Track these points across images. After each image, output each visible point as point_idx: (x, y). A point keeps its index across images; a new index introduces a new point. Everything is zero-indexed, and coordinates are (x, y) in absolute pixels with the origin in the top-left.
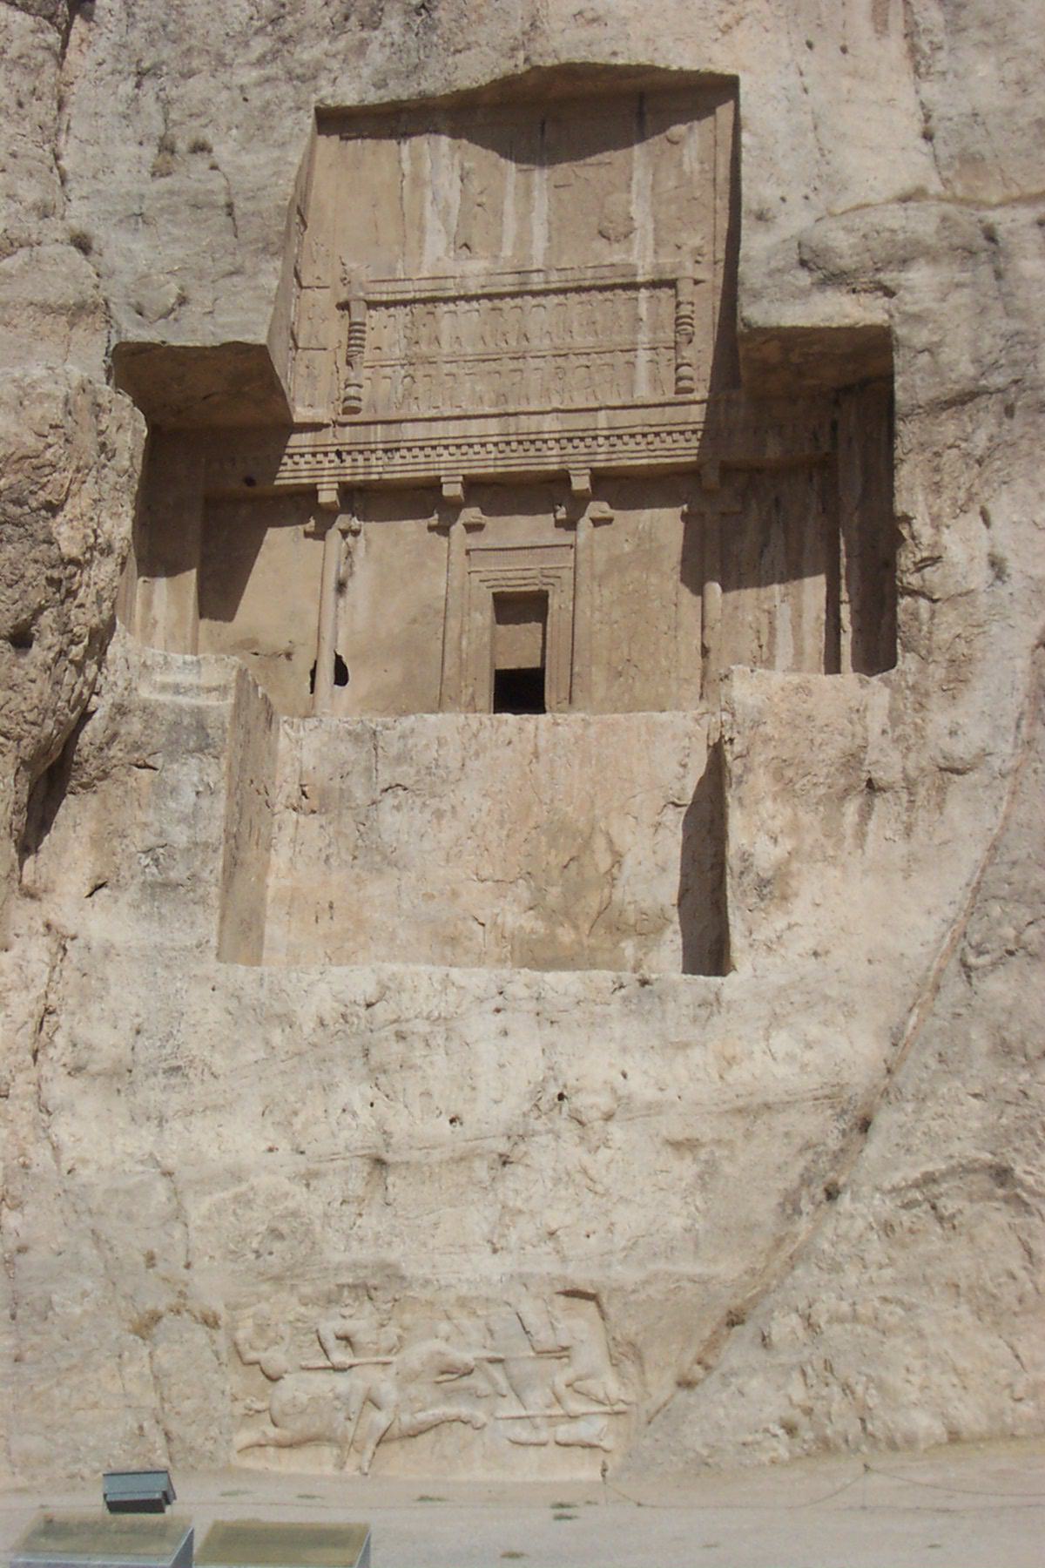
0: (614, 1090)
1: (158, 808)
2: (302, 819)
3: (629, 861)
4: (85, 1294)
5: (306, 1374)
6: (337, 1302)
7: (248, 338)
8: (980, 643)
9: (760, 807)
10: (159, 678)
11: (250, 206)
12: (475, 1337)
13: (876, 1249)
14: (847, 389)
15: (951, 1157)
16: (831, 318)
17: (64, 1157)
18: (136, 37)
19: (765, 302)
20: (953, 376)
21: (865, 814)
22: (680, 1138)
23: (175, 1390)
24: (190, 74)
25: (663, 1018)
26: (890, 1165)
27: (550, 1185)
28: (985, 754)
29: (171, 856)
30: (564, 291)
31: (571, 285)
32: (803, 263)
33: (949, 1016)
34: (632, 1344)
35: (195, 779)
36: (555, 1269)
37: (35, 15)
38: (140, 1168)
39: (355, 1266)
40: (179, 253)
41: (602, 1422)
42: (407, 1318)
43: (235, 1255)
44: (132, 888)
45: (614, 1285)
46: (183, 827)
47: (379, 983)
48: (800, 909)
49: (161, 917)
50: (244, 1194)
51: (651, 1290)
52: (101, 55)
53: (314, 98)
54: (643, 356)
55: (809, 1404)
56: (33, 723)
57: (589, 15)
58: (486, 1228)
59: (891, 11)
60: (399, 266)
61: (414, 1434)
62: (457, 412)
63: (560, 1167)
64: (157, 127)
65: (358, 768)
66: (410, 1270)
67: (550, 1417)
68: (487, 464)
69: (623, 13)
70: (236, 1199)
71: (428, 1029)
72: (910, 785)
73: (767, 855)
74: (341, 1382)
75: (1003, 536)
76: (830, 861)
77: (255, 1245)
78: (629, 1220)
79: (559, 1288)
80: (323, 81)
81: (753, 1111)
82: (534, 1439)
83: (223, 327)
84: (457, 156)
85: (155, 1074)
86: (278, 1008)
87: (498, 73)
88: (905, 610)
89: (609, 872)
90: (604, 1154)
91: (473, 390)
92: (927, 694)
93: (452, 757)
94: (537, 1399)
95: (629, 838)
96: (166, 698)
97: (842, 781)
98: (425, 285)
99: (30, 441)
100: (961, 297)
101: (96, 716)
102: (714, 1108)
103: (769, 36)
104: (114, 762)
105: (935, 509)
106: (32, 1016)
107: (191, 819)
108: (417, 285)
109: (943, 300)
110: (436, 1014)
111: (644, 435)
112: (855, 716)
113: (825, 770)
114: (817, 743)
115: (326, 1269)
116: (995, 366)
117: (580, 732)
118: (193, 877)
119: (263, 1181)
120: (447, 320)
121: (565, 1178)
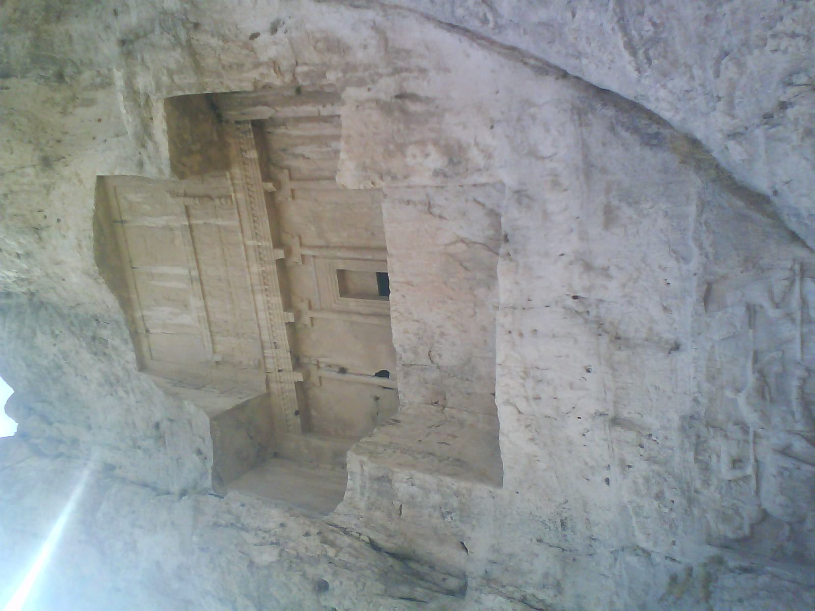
0: (571, 263)
8: (318, 35)
15: (613, 29)
16: (163, 131)
19: (162, 167)
20: (182, 61)
21: (414, 97)
24: (134, 424)
28: (375, 27)
29: (446, 504)
32: (143, 146)
35: (406, 485)
38: (618, 565)
42: (721, 417)
51: (707, 244)
54: (220, 222)
56: (364, 585)
58: (661, 355)
68: (277, 300)
70: (637, 514)
75: (261, 24)
77: (666, 510)
81: (588, 168)
85: (565, 536)
89: (467, 244)
90: (613, 271)
92: (348, 64)
100: (147, 57)
101: (372, 537)
110: (522, 374)
116: (176, 37)
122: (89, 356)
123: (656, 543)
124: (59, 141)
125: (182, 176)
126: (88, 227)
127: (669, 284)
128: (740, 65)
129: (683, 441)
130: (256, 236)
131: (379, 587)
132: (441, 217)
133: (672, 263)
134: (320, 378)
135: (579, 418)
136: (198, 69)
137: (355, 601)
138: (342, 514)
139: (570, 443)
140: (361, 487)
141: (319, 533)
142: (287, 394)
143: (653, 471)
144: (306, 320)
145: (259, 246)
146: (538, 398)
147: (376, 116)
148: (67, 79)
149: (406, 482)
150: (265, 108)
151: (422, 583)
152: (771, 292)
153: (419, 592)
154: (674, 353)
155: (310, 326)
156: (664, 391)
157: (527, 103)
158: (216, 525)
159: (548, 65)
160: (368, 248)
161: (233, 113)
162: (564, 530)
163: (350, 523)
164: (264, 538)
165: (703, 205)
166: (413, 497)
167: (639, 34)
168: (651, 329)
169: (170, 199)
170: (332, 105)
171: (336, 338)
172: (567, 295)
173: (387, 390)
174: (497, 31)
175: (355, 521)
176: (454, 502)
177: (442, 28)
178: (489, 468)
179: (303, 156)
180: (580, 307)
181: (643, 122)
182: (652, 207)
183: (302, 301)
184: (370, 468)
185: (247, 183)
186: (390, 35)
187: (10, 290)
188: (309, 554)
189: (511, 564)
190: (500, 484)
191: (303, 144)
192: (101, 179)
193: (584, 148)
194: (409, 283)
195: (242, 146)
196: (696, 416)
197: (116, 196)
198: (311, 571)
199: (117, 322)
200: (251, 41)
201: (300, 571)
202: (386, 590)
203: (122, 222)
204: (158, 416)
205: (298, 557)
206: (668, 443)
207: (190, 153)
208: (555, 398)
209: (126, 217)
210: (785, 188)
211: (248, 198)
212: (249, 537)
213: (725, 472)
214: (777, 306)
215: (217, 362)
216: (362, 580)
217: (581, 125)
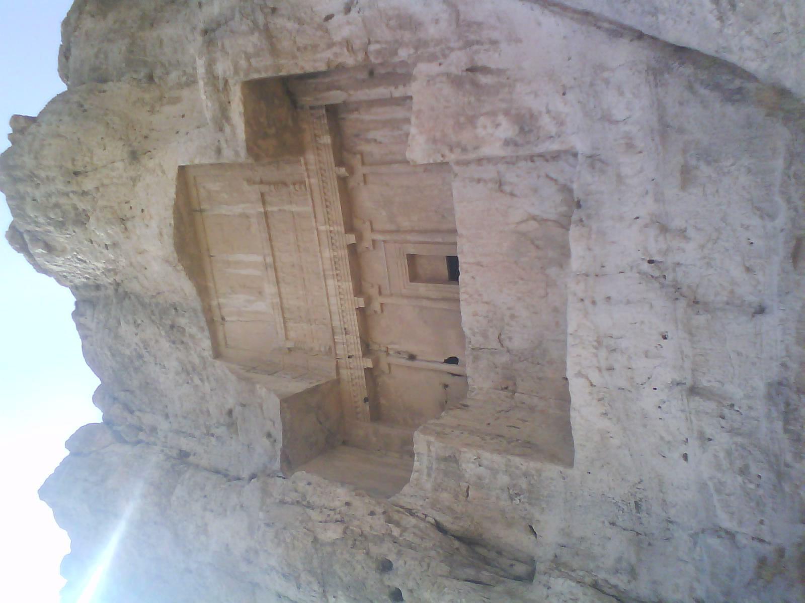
0: (646, 226)
2: (519, 390)
8: (391, 13)
10: (425, 477)
16: (240, 113)
19: (239, 149)
20: (259, 44)
21: (485, 70)
24: (208, 411)
29: (514, 486)
32: (221, 130)
54: (294, 208)
56: (429, 565)
68: (348, 285)
70: (718, 491)
79: (789, 266)
81: (664, 130)
85: (640, 518)
90: (691, 232)
100: (227, 43)
101: (438, 518)
110: (595, 344)
115: (772, 439)
116: (255, 22)
122: (168, 344)
123: (740, 523)
124: (146, 137)
127: (752, 243)
129: (770, 410)
130: (328, 221)
131: (444, 568)
132: (512, 195)
133: (755, 221)
134: (389, 365)
135: (655, 389)
136: (274, 51)
137: (420, 582)
138: (407, 496)
139: (645, 416)
140: (427, 468)
141: (384, 513)
142: (357, 380)
143: (736, 443)
144: (376, 306)
145: (331, 232)
146: (611, 369)
147: (447, 90)
148: (156, 80)
149: (473, 463)
150: (339, 92)
151: (487, 567)
153: (485, 575)
154: (759, 316)
156: (747, 357)
157: (600, 68)
158: (282, 502)
159: (623, 27)
160: (438, 231)
161: (308, 99)
162: (638, 512)
163: (417, 504)
164: (329, 515)
166: (480, 478)
169: (245, 186)
170: (404, 85)
171: (406, 323)
172: (643, 259)
175: (421, 502)
176: (523, 484)
178: (560, 446)
179: (375, 142)
180: (657, 272)
181: (724, 78)
182: (733, 165)
183: (372, 286)
184: (438, 447)
185: (321, 169)
186: (462, 8)
187: (98, 282)
189: (582, 548)
190: (571, 464)
192: (182, 169)
193: (660, 107)
194: (479, 264)
195: (316, 132)
198: (375, 550)
199: (195, 311)
200: (326, 23)
201: (365, 549)
202: (450, 572)
203: (201, 211)
204: (231, 402)
206: (753, 414)
208: (629, 368)
209: (204, 206)
211: (321, 183)
212: (315, 515)
215: (290, 349)
216: (427, 560)
217: (656, 86)
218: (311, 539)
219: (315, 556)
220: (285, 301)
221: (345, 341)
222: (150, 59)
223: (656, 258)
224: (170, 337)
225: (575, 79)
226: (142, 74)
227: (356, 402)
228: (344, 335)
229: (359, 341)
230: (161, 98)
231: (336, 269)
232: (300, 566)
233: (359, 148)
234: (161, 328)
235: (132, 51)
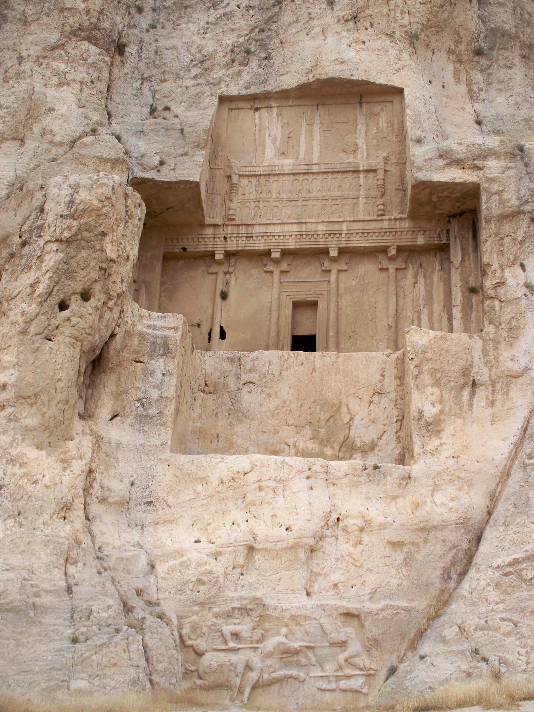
0: (363, 517)
1: (144, 381)
2: (205, 396)
3: (357, 419)
4: (109, 607)
5: (216, 653)
6: (231, 616)
7: (191, 179)
8: (522, 321)
9: (426, 390)
10: (146, 322)
11: (191, 130)
12: (299, 635)
13: (493, 595)
14: (454, 216)
16: (454, 178)
17: (96, 541)
18: (142, 65)
19: (424, 172)
20: (509, 205)
21: (473, 394)
22: (395, 540)
23: (155, 658)
24: (165, 81)
25: (385, 485)
26: (494, 556)
27: (333, 561)
29: (150, 403)
30: (327, 173)
31: (329, 170)
32: (441, 156)
33: (517, 487)
34: (376, 640)
35: (162, 368)
36: (339, 603)
37: (100, 48)
38: (133, 548)
39: (241, 598)
40: (161, 147)
41: (361, 680)
42: (267, 625)
43: (181, 591)
44: (131, 418)
45: (367, 610)
46: (156, 390)
47: (251, 463)
48: (446, 436)
49: (144, 431)
50: (185, 562)
51: (385, 613)
52: (126, 71)
53: (219, 91)
54: (362, 201)
55: (471, 670)
56: (89, 334)
57: (341, 60)
58: (303, 582)
59: (461, 74)
60: (254, 161)
61: (270, 683)
62: (279, 221)
63: (338, 553)
64: (150, 100)
65: (232, 374)
66: (267, 602)
67: (337, 676)
68: (292, 244)
69: (355, 60)
70: (181, 564)
71: (275, 485)
72: (493, 383)
73: (430, 412)
74: (233, 658)
76: (459, 416)
77: (191, 587)
78: (372, 580)
79: (340, 611)
80: (223, 85)
81: (427, 529)
82: (328, 687)
83: (179, 174)
84: (280, 118)
85: (140, 505)
86: (201, 474)
87: (300, 82)
88: (488, 306)
90: (360, 547)
91: (286, 213)
92: (499, 343)
93: (275, 369)
94: (330, 668)
95: (358, 408)
96: (149, 331)
97: (462, 380)
98: (265, 169)
99: (96, 202)
100: (512, 172)
101: (118, 336)
102: (410, 527)
103: (415, 75)
104: (125, 358)
105: (501, 262)
106: (83, 471)
107: (160, 386)
108: (261, 169)
109: (503, 173)
110: (279, 478)
111: (363, 233)
112: (467, 351)
113: (454, 375)
114: (450, 362)
115: (226, 600)
116: (527, 202)
117: (335, 360)
118: (160, 413)
119: (194, 556)
120: (275, 185)
121: (341, 559)
122: (229, 42)
125: (414, 187)
126: (359, 75)
128: (508, 634)
133: (368, 590)
134: (216, 273)
137: (77, 327)
142: (203, 243)
144: (270, 267)
148: (477, 58)
149: (165, 369)
150: (460, 258)
152: (355, 656)
155: (265, 269)
160: (338, 332)
161: (456, 230)
165: (408, 610)
167: (523, 569)
168: (320, 574)
173: (208, 336)
174: (522, 465)
175: (129, 321)
177: (524, 423)
181: (459, 569)
182: (403, 575)
185: (396, 232)
186: (520, 381)
188: (111, 285)
191: (426, 284)
192: (400, 91)
194: (314, 370)
195: (428, 232)
196: (266, 608)
197: (384, 101)
199: (265, 81)
200: (519, 263)
202: (84, 352)
203: (361, 103)
205: (109, 275)
207: (431, 194)
210: (429, 663)
213: (227, 629)
214: (346, 660)
215: (229, 177)
218: (105, 230)
219: (92, 234)
220: (276, 178)
221: (240, 235)
222: (495, 53)
223: (341, 524)
224: (237, 47)
225: (463, 465)
226: (483, 44)
227: (182, 239)
228: (245, 235)
229: (239, 249)
230: (460, 61)
231: (307, 235)
232: (82, 221)
233: (410, 266)
234: (246, 38)
235: (503, 36)
